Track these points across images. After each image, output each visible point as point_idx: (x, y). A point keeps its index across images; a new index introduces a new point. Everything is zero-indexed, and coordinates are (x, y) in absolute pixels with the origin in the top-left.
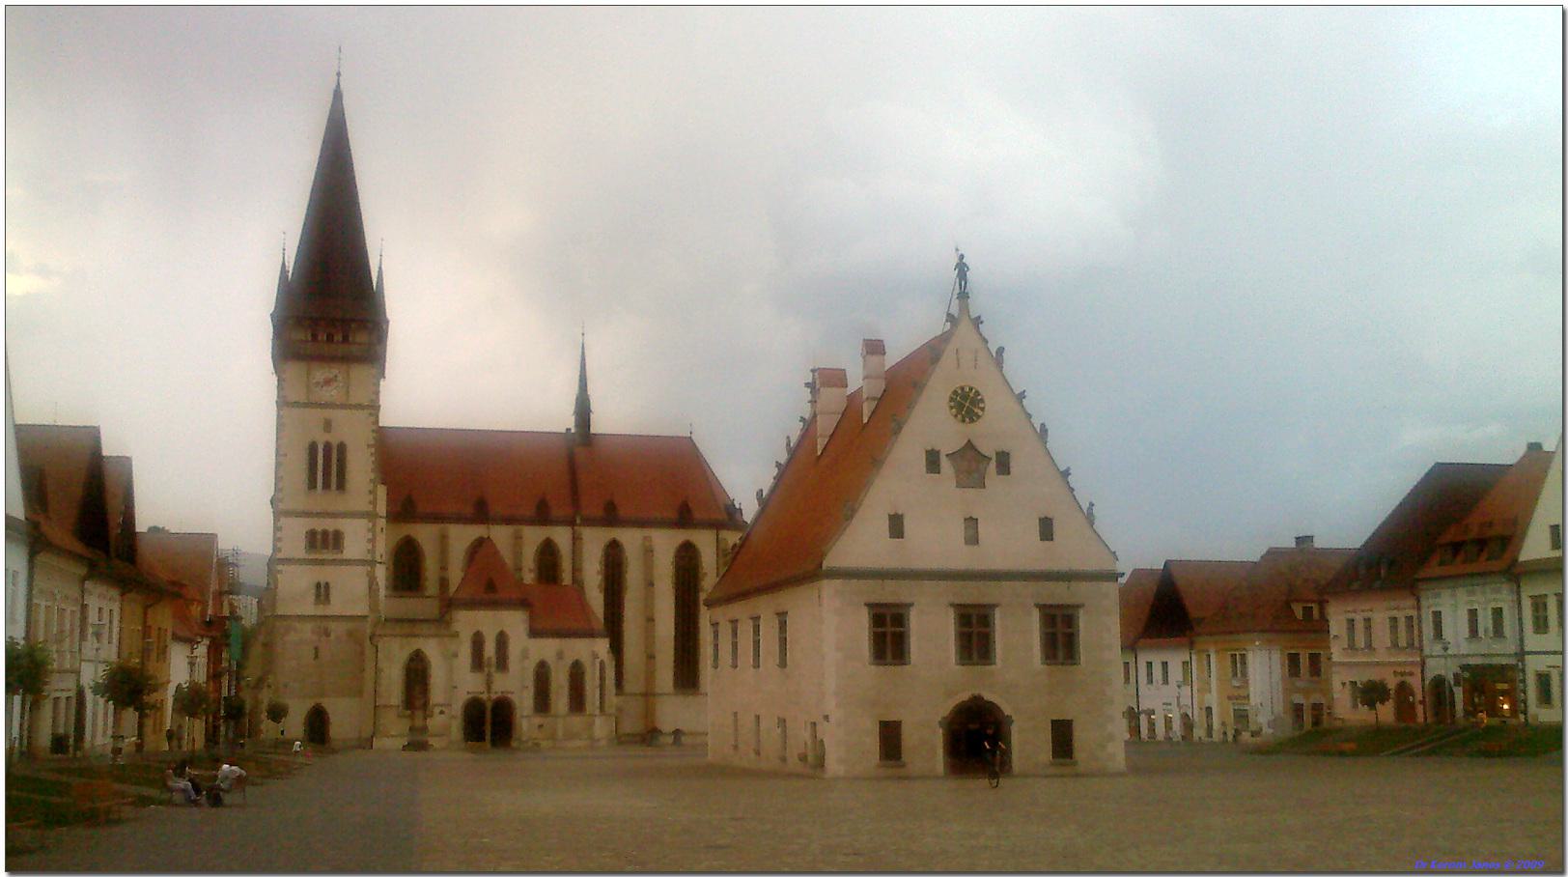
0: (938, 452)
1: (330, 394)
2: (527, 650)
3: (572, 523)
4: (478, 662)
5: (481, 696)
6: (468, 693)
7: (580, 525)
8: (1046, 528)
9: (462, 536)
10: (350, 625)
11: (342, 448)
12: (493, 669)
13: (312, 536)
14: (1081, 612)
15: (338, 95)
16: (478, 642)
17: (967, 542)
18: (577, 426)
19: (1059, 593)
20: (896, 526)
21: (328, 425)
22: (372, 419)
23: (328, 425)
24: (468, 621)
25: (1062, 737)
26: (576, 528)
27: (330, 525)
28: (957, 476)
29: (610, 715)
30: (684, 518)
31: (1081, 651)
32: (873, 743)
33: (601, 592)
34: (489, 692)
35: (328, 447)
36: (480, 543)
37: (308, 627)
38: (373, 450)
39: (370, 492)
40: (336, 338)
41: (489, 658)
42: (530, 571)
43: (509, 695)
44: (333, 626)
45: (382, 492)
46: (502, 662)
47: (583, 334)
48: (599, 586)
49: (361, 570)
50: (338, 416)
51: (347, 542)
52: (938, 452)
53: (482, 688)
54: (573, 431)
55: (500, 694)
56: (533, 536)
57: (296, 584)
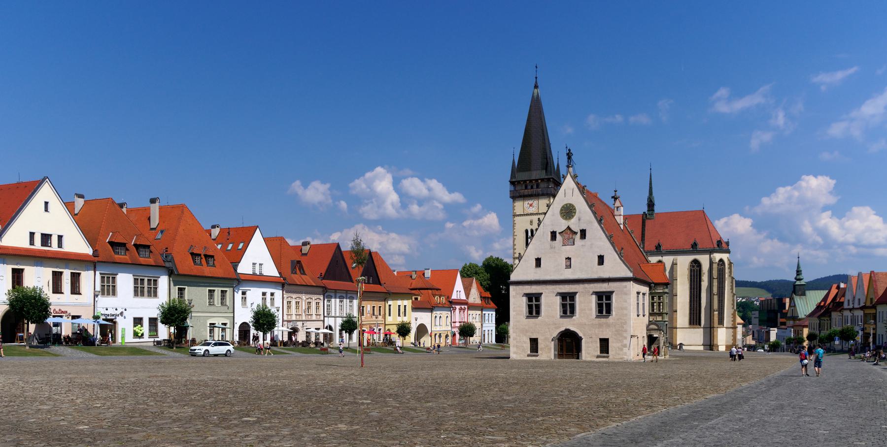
1: (532, 210)
20: (538, 262)
21: (531, 222)
25: (604, 344)
30: (694, 248)
31: (613, 309)
32: (527, 345)
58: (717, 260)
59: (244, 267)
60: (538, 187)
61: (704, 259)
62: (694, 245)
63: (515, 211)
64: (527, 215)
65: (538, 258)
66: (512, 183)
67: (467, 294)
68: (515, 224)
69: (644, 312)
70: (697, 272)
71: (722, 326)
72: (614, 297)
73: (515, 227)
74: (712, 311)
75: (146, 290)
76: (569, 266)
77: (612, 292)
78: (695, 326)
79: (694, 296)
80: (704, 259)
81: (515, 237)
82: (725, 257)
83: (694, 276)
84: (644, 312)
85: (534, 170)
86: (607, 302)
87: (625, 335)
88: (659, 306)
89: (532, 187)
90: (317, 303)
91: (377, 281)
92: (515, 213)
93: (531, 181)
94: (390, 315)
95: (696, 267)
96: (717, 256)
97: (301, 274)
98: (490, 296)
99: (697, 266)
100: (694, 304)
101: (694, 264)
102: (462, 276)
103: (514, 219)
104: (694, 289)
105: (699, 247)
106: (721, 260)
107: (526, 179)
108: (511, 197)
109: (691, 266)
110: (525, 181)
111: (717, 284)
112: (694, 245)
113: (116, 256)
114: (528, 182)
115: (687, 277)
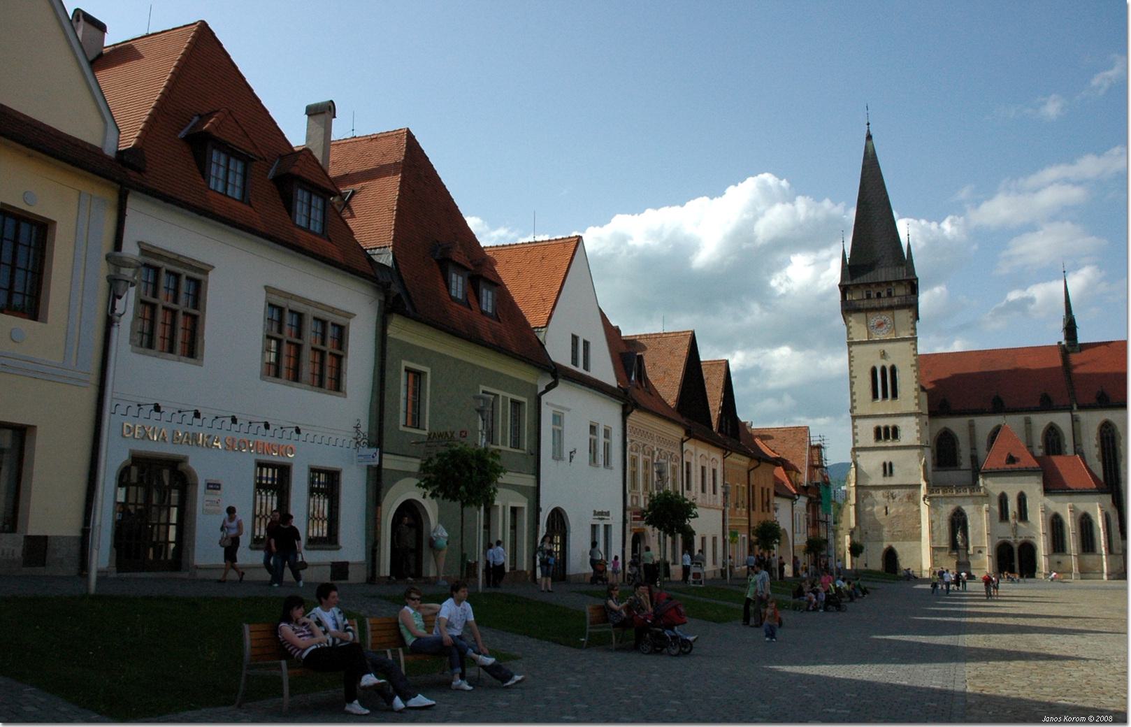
2: (1040, 505)
3: (1070, 409)
4: (1004, 515)
5: (1008, 540)
6: (999, 538)
7: (1076, 411)
9: (986, 424)
10: (908, 491)
11: (893, 369)
12: (1017, 522)
13: (878, 430)
15: (869, 137)
16: (1003, 499)
18: (1067, 339)
21: (884, 355)
22: (913, 346)
23: (884, 355)
24: (993, 486)
26: (1074, 414)
27: (890, 422)
29: (1117, 555)
33: (1099, 461)
34: (1015, 537)
35: (884, 369)
36: (997, 430)
37: (880, 493)
38: (915, 368)
39: (916, 397)
40: (882, 296)
41: (1015, 512)
42: (1040, 447)
43: (1032, 540)
44: (896, 491)
45: (924, 396)
46: (1023, 515)
47: (1064, 272)
48: (1097, 456)
49: (916, 452)
50: (887, 347)
51: (902, 433)
53: (1010, 534)
54: (1064, 343)
55: (1023, 539)
56: (1041, 421)
57: (871, 463)
60: (889, 294)
63: (850, 336)
64: (875, 342)
66: (844, 289)
68: (853, 357)
73: (852, 363)
81: (854, 380)
89: (879, 295)
90: (674, 469)
92: (852, 339)
93: (878, 284)
94: (754, 510)
103: (851, 349)
107: (869, 281)
110: (868, 285)
114: (873, 286)
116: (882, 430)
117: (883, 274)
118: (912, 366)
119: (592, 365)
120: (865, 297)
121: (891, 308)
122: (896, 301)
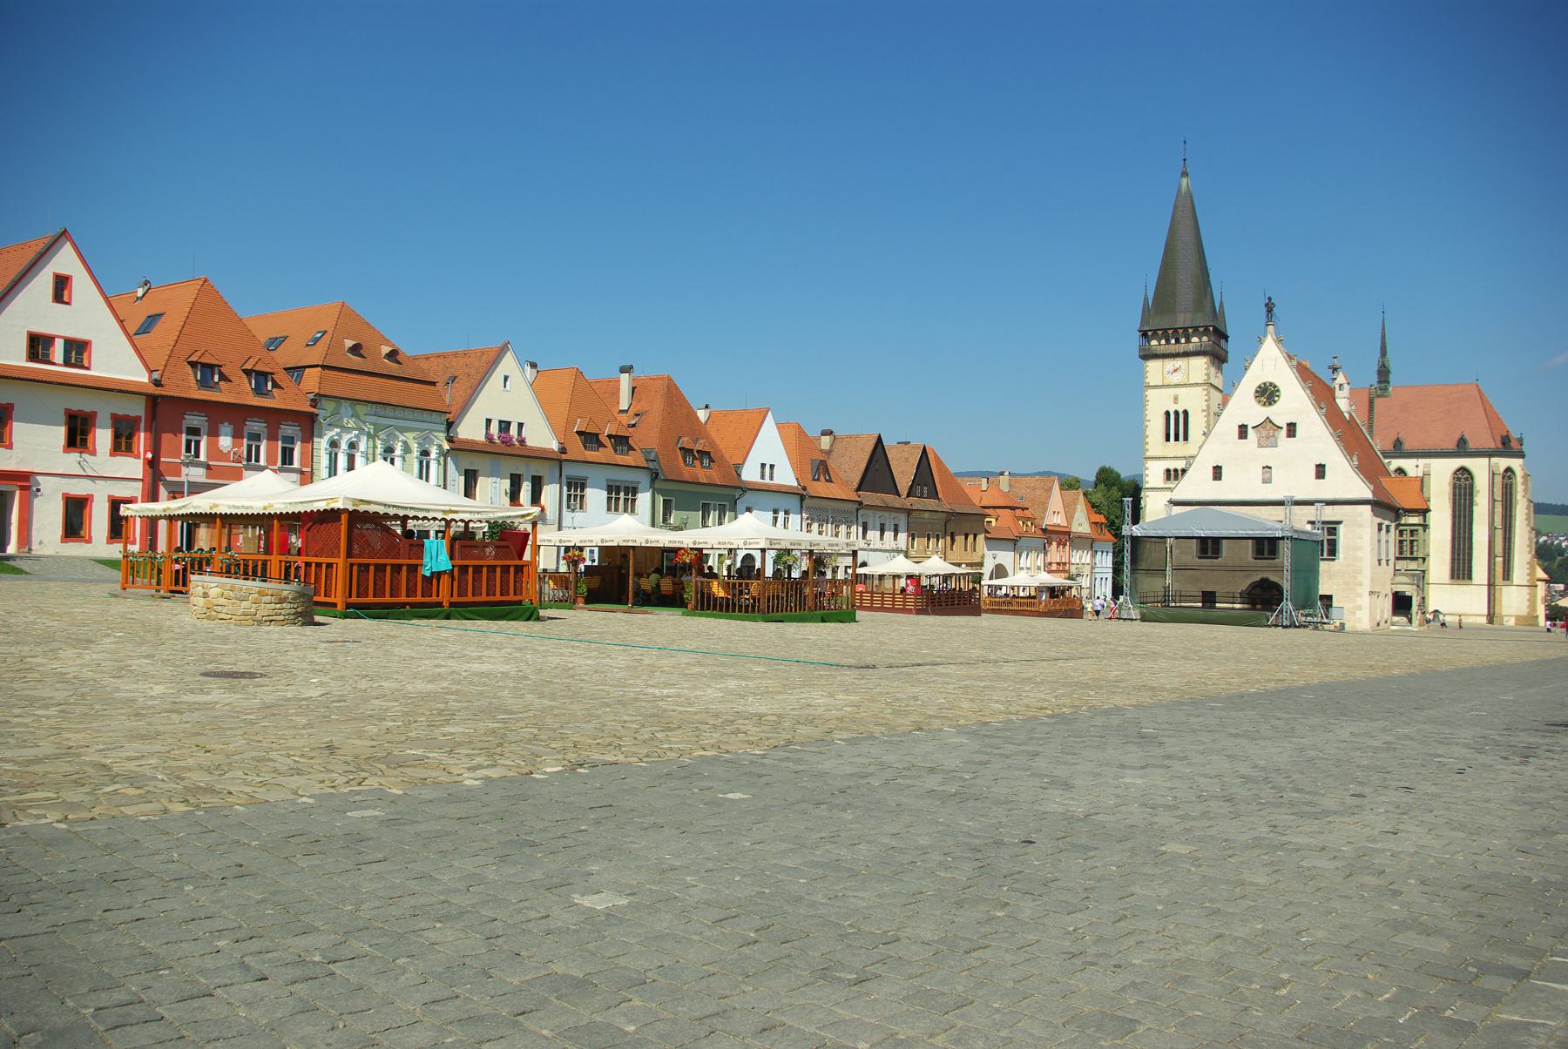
0: (1247, 426)
8: (1320, 471)
11: (1186, 413)
13: (1168, 471)
14: (1341, 526)
17: (1265, 481)
19: (1330, 513)
20: (1217, 473)
21: (1176, 399)
22: (1205, 392)
23: (1176, 399)
28: (1259, 440)
35: (1177, 413)
38: (1205, 413)
50: (1180, 391)
52: (1247, 426)
58: (1502, 470)
59: (750, 474)
61: (1480, 468)
62: (1462, 442)
63: (1147, 381)
64: (1169, 386)
65: (1217, 466)
66: (1144, 334)
67: (1070, 518)
68: (1148, 401)
69: (1387, 555)
70: (1465, 488)
71: (1509, 582)
72: (1341, 529)
73: (1147, 407)
74: (1493, 556)
75: (621, 502)
76: (1267, 481)
77: (1339, 523)
78: (1460, 582)
79: (1459, 529)
80: (1480, 468)
82: (1516, 464)
83: (1460, 495)
84: (1387, 555)
85: (1182, 312)
86: (1330, 537)
87: (1359, 591)
88: (1412, 548)
89: (1177, 341)
91: (934, 494)
93: (1175, 330)
95: (1463, 480)
96: (1502, 463)
97: (827, 481)
98: (1104, 521)
99: (1466, 479)
100: (1459, 545)
101: (1460, 476)
102: (1062, 488)
103: (1147, 393)
104: (1459, 517)
105: (1471, 445)
106: (1509, 470)
108: (1140, 357)
109: (1454, 478)
110: (1165, 331)
111: (1501, 510)
112: (1462, 442)
113: (587, 452)
114: (1170, 332)
115: (1447, 496)
116: (1172, 473)
117: (1182, 320)
118: (1203, 411)
119: (775, 478)
120: (1163, 342)
121: (1186, 354)
122: (1191, 347)
